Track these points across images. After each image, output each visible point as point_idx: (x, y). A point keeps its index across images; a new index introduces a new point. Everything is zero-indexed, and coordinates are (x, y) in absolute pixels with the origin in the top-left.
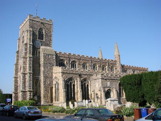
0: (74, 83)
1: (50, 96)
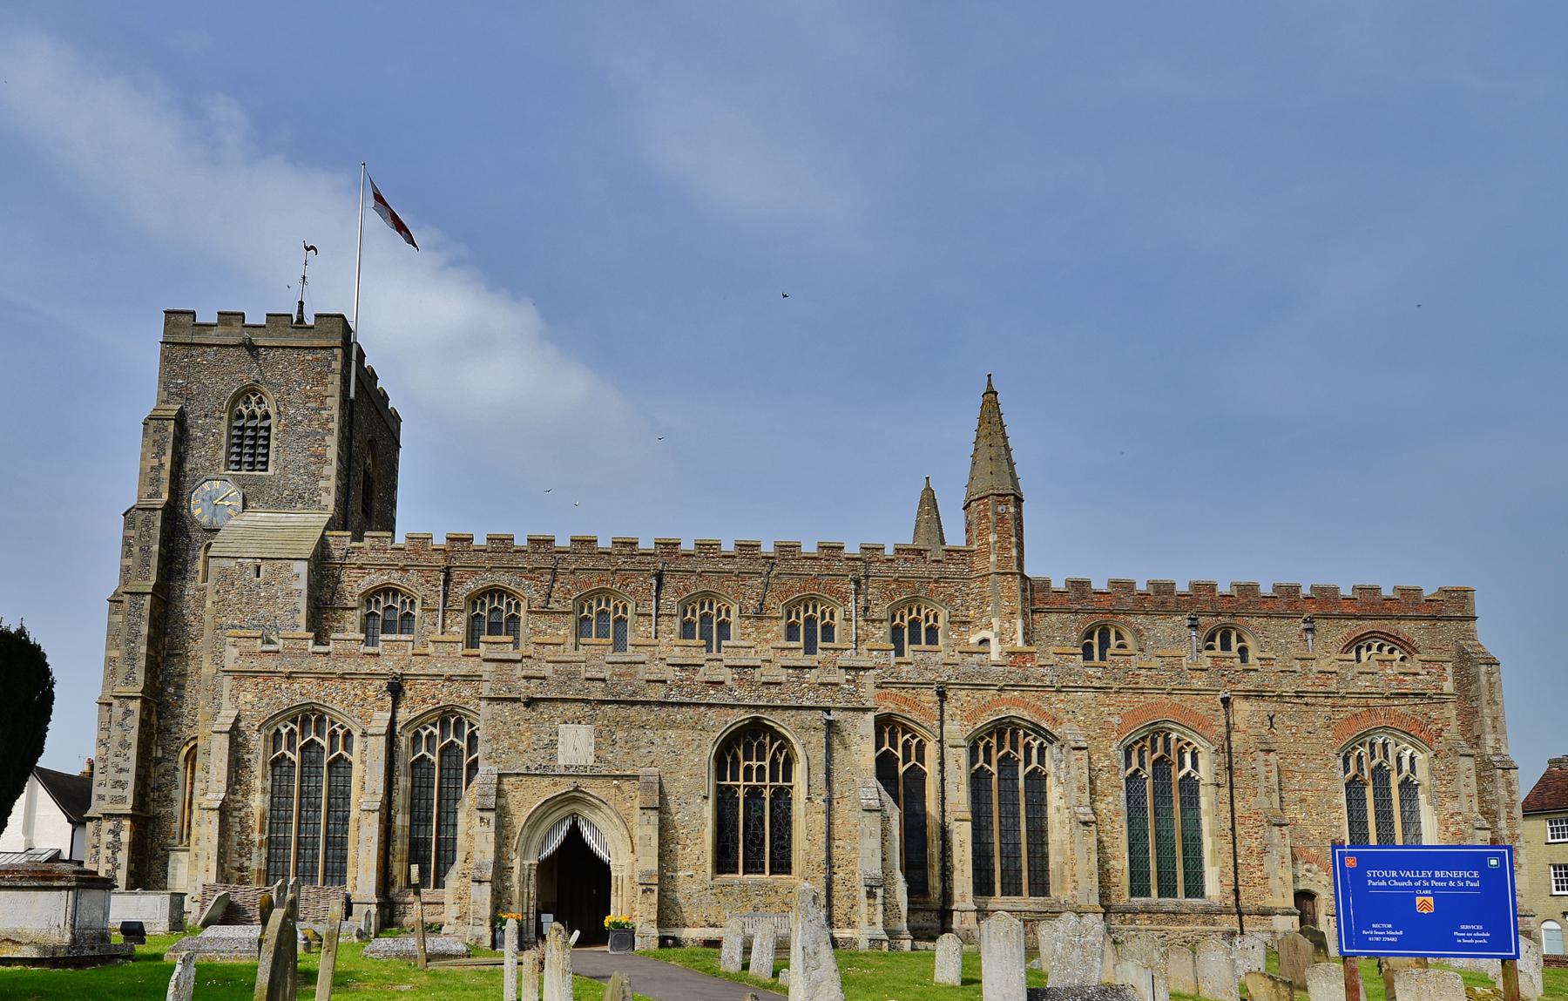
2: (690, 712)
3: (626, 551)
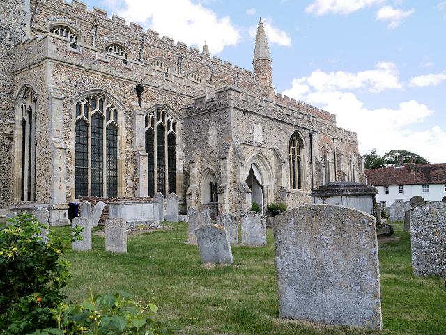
3: (169, 43)
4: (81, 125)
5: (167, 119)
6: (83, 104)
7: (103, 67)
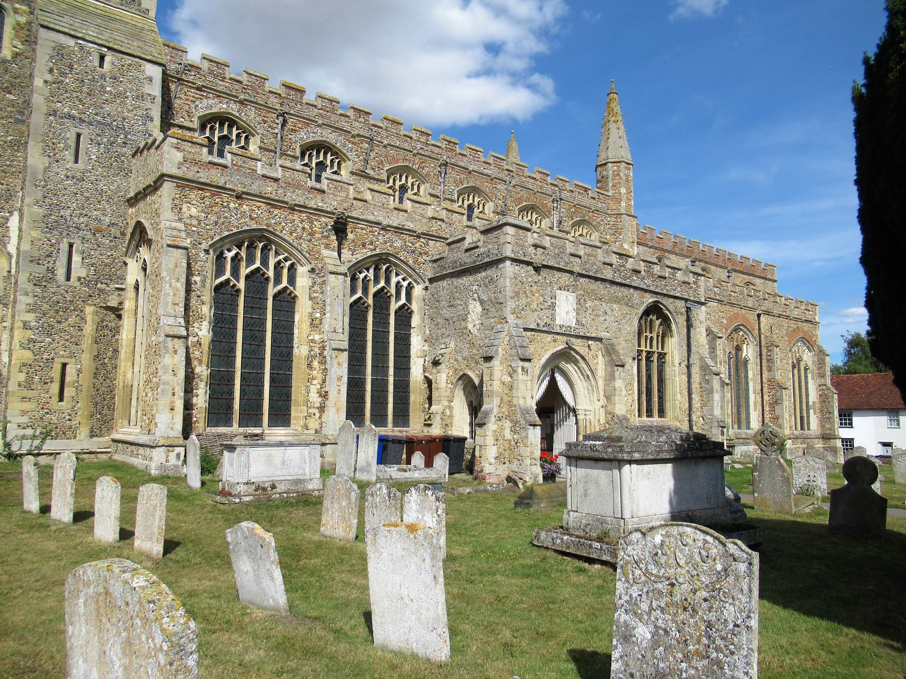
0: (292, 280)
1: (86, 380)
2: (625, 291)
4: (224, 295)
5: (394, 280)
6: (229, 255)
7: (269, 189)
